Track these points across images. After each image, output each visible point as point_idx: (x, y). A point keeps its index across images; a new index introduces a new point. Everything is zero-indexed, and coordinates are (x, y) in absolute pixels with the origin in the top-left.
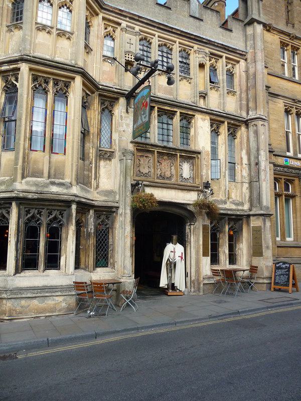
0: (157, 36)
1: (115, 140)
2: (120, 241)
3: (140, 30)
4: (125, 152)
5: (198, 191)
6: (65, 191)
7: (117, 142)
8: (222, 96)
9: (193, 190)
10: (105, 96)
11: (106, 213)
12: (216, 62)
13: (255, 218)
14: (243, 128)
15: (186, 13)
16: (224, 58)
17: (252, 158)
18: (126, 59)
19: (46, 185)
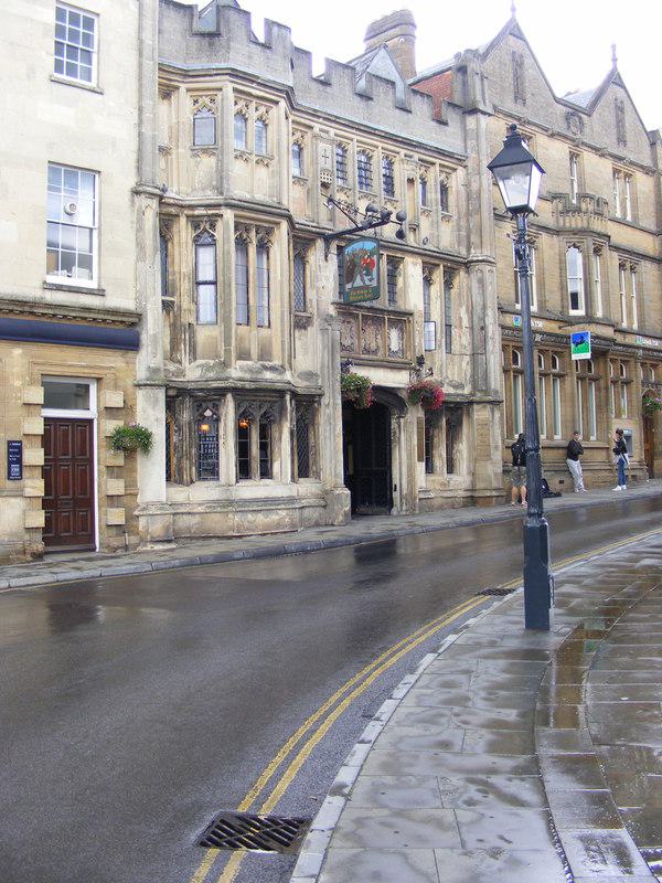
2: (328, 441)
4: (328, 319)
5: (410, 369)
6: (279, 378)
7: (315, 303)
8: (435, 225)
9: (404, 369)
10: (299, 237)
11: (307, 404)
13: (481, 406)
14: (462, 273)
15: (390, 103)
16: (437, 166)
17: (475, 319)
19: (259, 371)
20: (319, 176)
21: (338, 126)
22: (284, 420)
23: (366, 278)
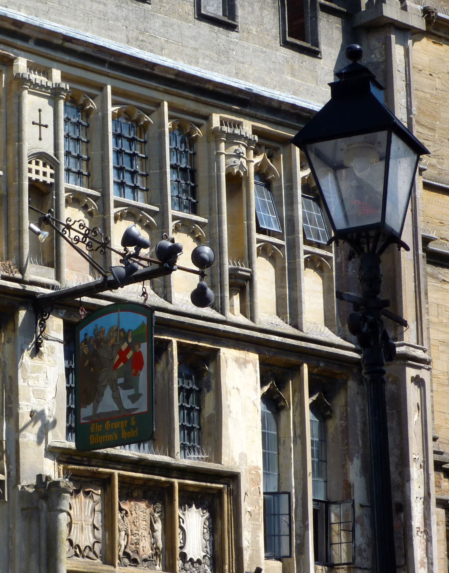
20: (26, 166)
21: (67, 58)
23: (124, 394)
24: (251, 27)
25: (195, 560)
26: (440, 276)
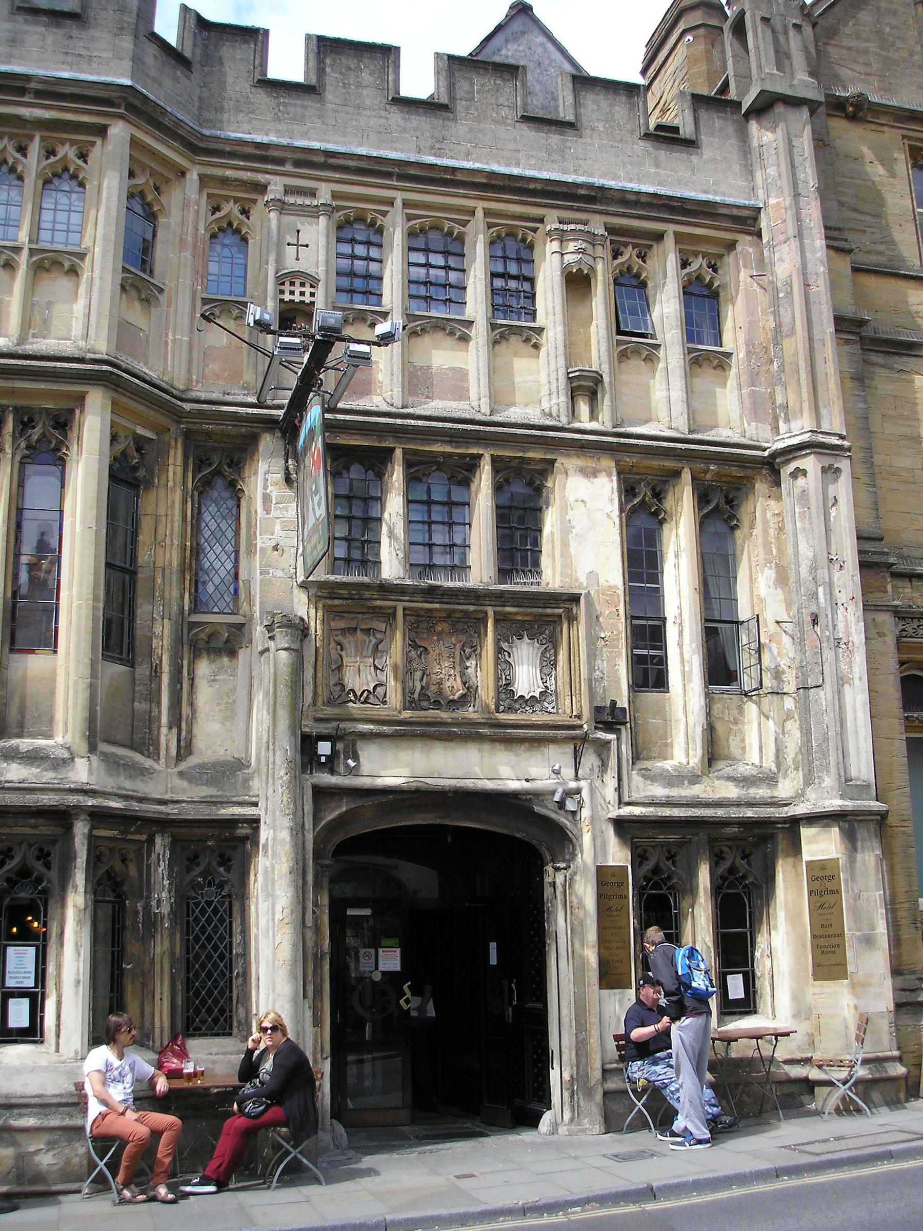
0: (398, 203)
1: (248, 583)
3: (335, 195)
6: (49, 776)
12: (643, 257)
18: (282, 301)
22: (70, 889)
24: (596, 124)
25: (527, 697)
26: (896, 366)
